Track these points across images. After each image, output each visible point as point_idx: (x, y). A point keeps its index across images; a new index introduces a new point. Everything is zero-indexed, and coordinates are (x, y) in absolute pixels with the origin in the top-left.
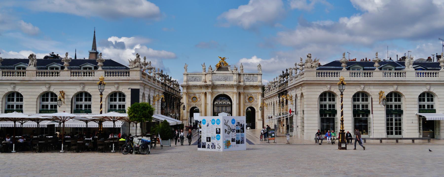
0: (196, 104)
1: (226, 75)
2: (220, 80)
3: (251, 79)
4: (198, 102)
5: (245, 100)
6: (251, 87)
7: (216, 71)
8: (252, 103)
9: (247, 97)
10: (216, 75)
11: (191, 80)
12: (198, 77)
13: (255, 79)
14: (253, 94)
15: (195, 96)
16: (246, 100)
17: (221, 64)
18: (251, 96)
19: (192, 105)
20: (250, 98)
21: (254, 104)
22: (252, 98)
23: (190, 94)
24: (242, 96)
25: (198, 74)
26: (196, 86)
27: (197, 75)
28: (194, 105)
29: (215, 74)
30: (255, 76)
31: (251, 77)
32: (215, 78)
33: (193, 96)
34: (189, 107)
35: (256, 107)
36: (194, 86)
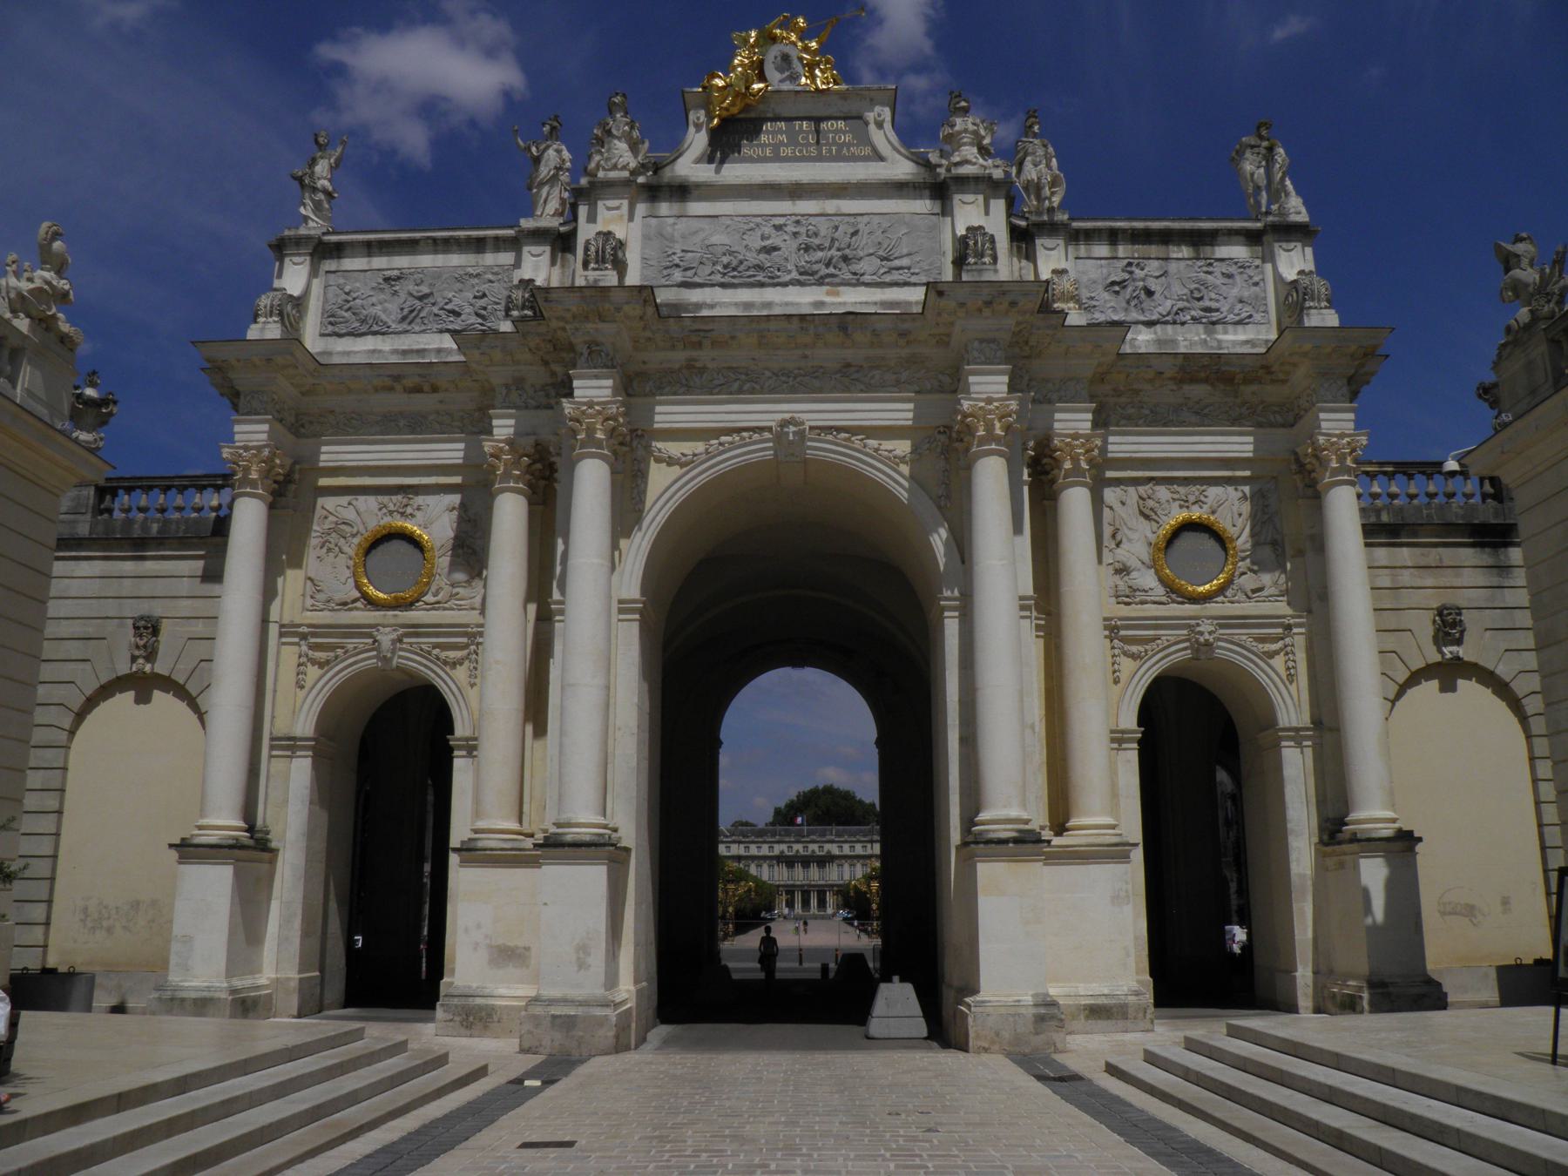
0: (415, 630)
1: (831, 206)
2: (759, 267)
3: (1178, 290)
4: (434, 606)
5: (1123, 570)
6: (1193, 380)
7: (698, 161)
8: (1213, 608)
9: (1145, 528)
10: (696, 207)
11: (377, 310)
12: (462, 278)
13: (1235, 292)
14: (1214, 492)
15: (411, 526)
16: (1133, 562)
17: (762, 77)
18: (1196, 513)
19: (351, 643)
20: (1188, 541)
21: (1243, 621)
22: (1209, 544)
23: (344, 500)
24: (1075, 502)
25: (457, 241)
26: (418, 390)
27: (455, 260)
28: (386, 638)
29: (682, 191)
30: (1223, 251)
31: (1173, 267)
32: (678, 248)
33: (370, 514)
34: (313, 672)
35: (1279, 662)
36: (391, 389)
